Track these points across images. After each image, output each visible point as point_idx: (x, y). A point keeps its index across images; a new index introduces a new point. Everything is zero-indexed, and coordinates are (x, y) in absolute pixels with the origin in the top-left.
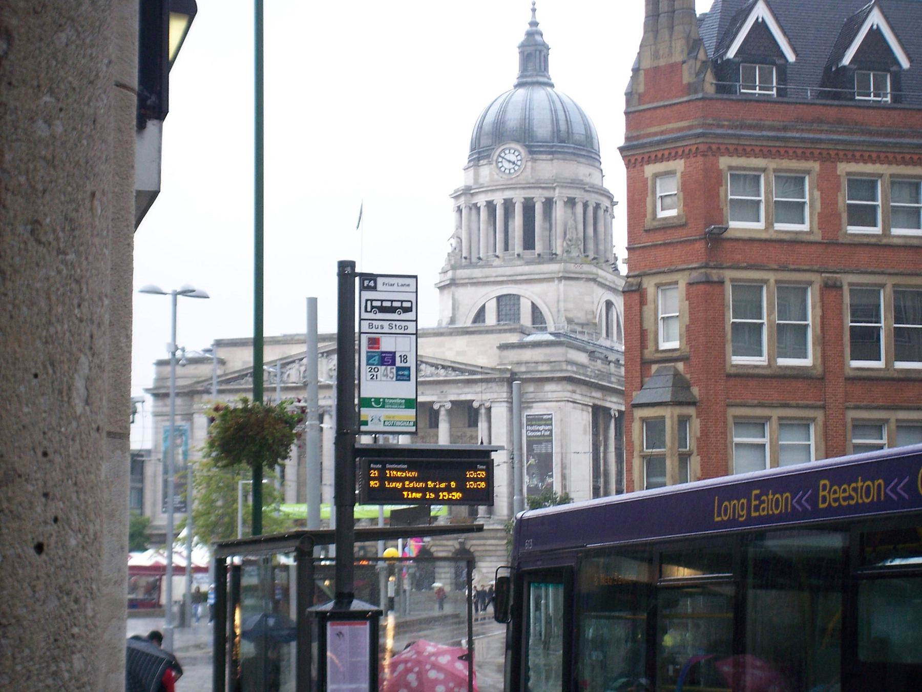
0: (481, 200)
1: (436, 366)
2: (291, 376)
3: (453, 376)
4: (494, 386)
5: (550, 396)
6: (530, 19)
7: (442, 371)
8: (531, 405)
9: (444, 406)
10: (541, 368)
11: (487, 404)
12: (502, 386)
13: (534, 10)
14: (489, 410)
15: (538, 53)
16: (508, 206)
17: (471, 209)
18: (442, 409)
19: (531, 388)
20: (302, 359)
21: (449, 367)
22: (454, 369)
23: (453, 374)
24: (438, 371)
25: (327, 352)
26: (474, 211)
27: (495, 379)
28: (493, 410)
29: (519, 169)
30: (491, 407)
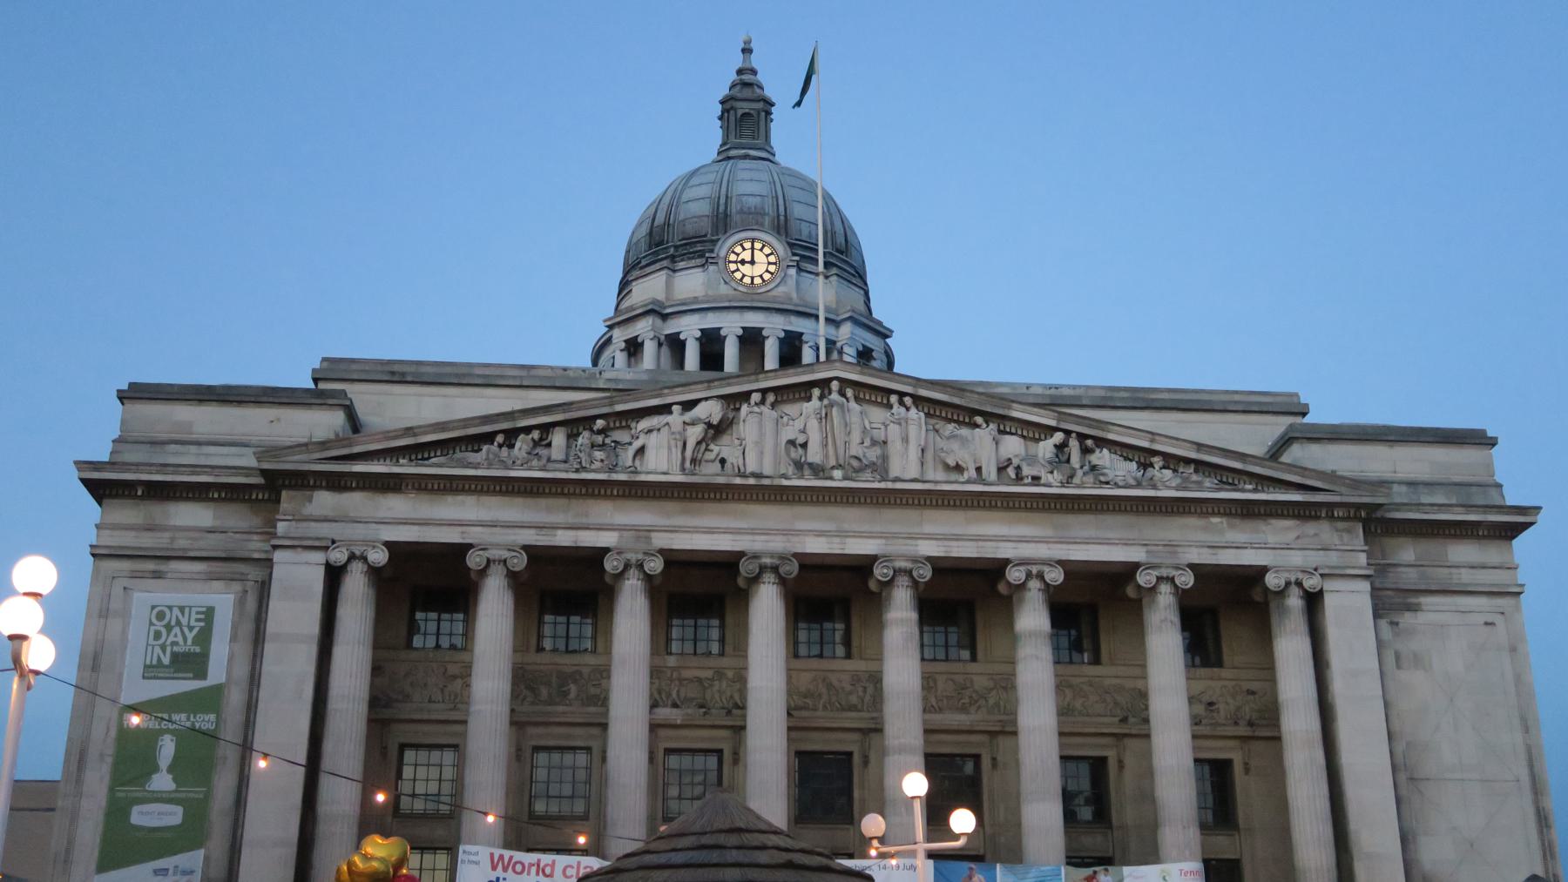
0: (689, 328)
1: (1143, 457)
2: (650, 455)
3: (1208, 490)
4: (1323, 531)
5: (1466, 577)
6: (739, 65)
7: (1168, 473)
8: (1413, 600)
9: (1171, 580)
10: (1426, 499)
11: (1311, 583)
12: (1348, 531)
13: (747, 51)
14: (1313, 601)
15: (763, 114)
16: (751, 340)
17: (660, 345)
18: (1165, 588)
19: (1407, 552)
20: (689, 405)
21: (1188, 461)
22: (1200, 465)
23: (1208, 483)
24: (1150, 471)
25: (775, 390)
26: (665, 350)
27: (1331, 506)
28: (1330, 601)
29: (771, 281)
30: (1321, 592)
